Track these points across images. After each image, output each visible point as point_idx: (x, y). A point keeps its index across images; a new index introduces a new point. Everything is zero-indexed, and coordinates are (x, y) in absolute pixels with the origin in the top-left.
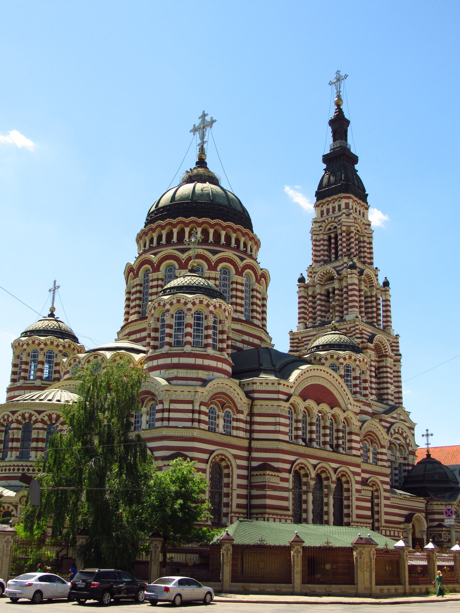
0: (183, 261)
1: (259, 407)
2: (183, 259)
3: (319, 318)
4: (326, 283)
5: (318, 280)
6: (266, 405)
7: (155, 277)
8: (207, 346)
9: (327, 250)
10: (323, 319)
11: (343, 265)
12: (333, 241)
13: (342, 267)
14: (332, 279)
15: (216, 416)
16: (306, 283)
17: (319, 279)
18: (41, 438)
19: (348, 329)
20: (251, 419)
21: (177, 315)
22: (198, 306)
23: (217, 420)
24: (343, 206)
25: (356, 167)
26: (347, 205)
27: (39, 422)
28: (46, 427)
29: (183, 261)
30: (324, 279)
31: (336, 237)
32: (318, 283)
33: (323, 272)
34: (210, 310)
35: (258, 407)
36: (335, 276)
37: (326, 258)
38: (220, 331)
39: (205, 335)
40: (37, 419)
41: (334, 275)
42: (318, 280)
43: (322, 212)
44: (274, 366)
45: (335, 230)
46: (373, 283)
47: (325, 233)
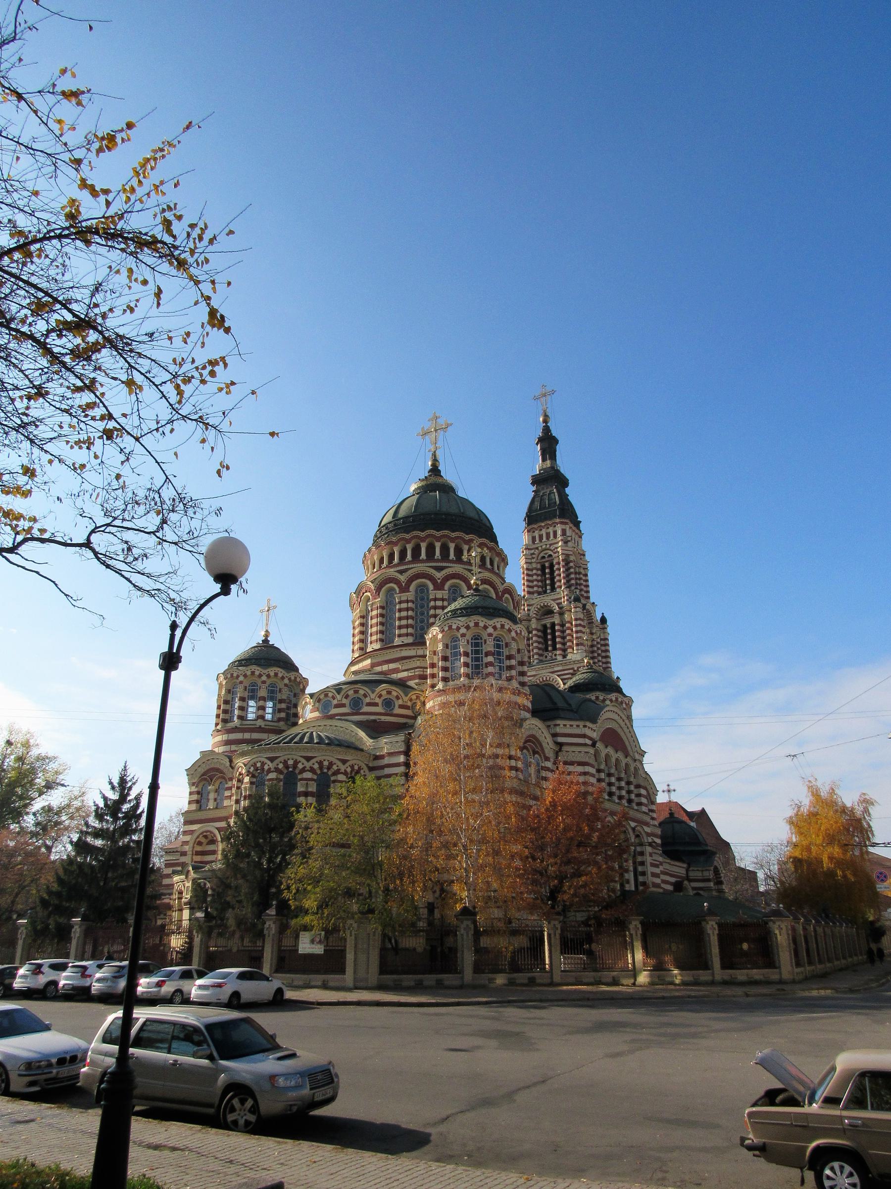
0: (439, 581)
1: (564, 753)
2: (439, 579)
3: (536, 657)
7: (403, 599)
9: (541, 581)
10: (541, 658)
12: (547, 571)
14: (549, 612)
19: (576, 669)
24: (559, 533)
25: (567, 490)
26: (564, 532)
27: (308, 770)
28: (315, 777)
29: (439, 581)
30: (540, 612)
31: (552, 566)
32: (534, 617)
37: (540, 589)
39: (507, 666)
40: (305, 767)
43: (534, 539)
44: (570, 705)
45: (550, 559)
47: (538, 561)
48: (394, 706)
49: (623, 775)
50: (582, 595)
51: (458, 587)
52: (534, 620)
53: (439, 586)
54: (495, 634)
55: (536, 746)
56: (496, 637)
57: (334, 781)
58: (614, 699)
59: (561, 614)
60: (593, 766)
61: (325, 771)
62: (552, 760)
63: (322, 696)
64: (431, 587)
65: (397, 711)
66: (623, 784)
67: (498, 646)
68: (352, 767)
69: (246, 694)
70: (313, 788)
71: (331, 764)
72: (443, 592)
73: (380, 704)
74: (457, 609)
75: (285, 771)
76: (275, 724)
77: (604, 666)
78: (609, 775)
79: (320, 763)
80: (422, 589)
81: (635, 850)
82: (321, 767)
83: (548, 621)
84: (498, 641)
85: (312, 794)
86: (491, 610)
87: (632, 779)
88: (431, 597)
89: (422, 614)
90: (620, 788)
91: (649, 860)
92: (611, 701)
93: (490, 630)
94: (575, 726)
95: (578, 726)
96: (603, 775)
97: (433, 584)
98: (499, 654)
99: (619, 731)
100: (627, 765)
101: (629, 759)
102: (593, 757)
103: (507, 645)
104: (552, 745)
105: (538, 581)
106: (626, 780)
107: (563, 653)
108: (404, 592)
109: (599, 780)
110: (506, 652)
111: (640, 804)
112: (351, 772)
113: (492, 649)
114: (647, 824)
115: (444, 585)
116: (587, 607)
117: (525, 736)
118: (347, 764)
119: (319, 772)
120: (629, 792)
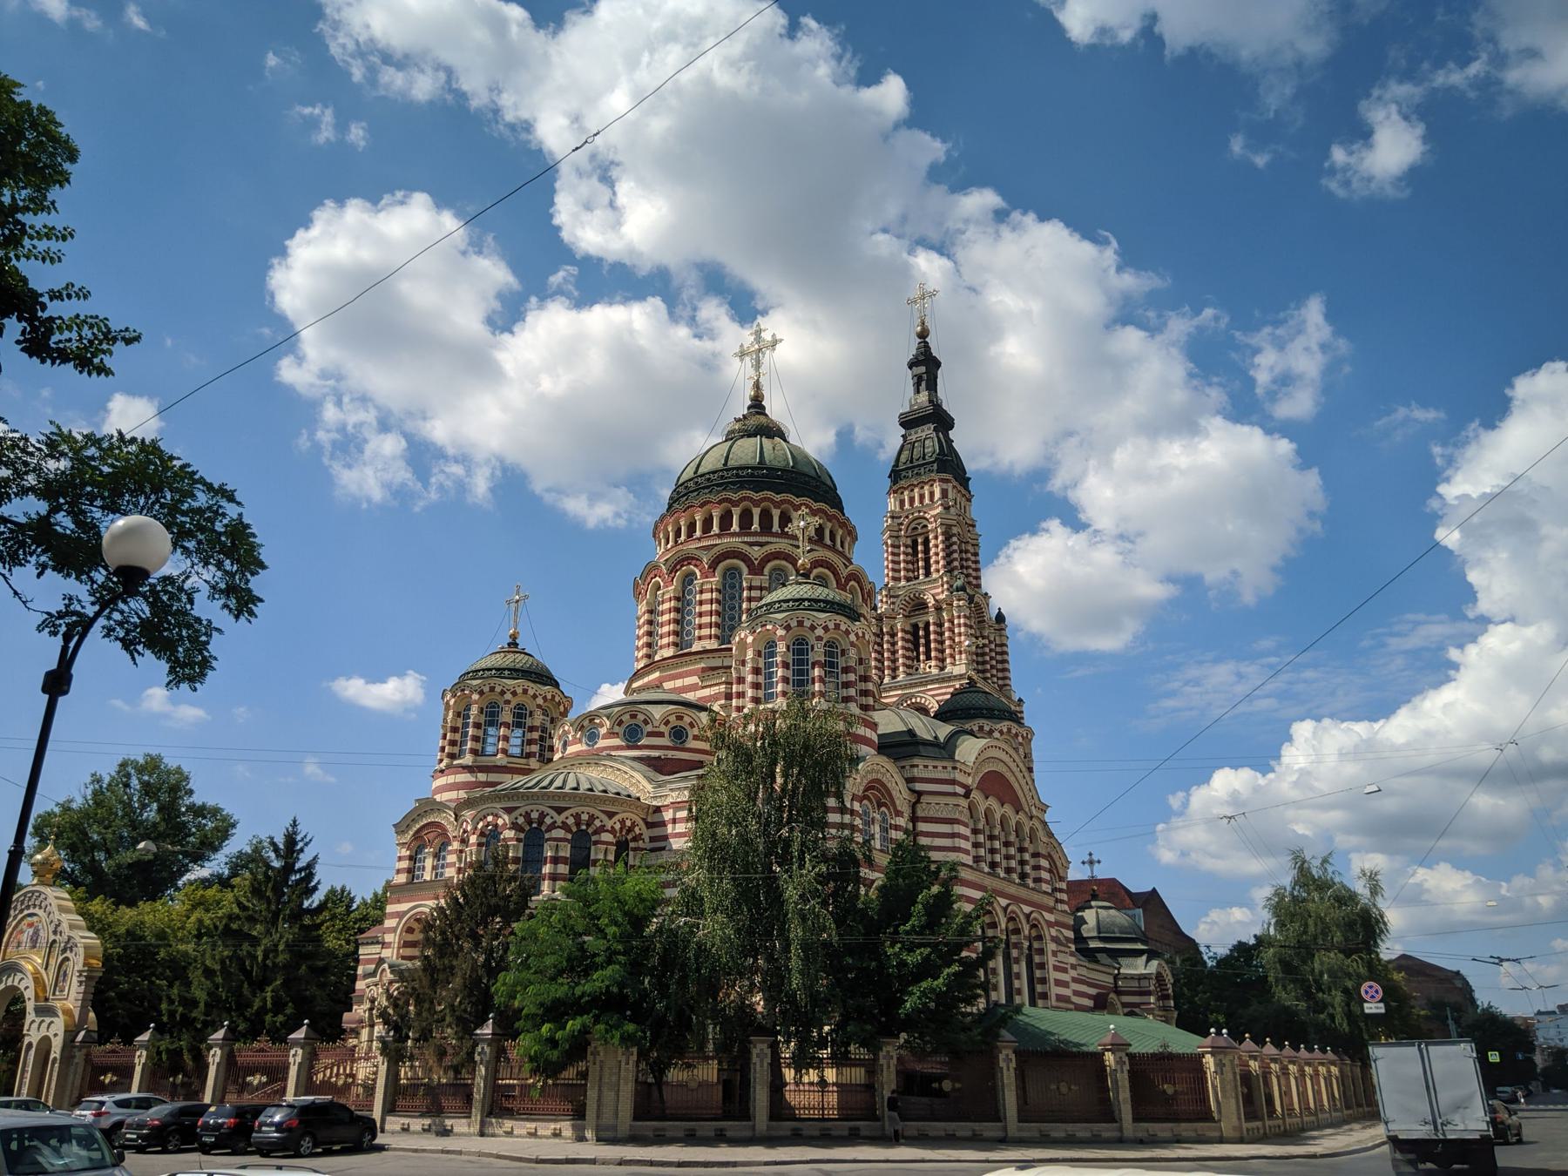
49: (1012, 838)
60: (966, 825)
63: (586, 723)
66: (1012, 851)
69: (482, 719)
73: (667, 734)
74: (775, 603)
76: (523, 761)
78: (992, 838)
81: (1030, 947)
87: (1027, 844)
90: (1008, 857)
91: (1052, 961)
93: (819, 632)
98: (832, 665)
99: (1008, 775)
100: (1018, 823)
101: (1021, 816)
102: (966, 812)
103: (843, 652)
106: (1017, 845)
110: (842, 662)
111: (1038, 880)
113: (822, 659)
114: (1051, 910)
120: (1022, 863)
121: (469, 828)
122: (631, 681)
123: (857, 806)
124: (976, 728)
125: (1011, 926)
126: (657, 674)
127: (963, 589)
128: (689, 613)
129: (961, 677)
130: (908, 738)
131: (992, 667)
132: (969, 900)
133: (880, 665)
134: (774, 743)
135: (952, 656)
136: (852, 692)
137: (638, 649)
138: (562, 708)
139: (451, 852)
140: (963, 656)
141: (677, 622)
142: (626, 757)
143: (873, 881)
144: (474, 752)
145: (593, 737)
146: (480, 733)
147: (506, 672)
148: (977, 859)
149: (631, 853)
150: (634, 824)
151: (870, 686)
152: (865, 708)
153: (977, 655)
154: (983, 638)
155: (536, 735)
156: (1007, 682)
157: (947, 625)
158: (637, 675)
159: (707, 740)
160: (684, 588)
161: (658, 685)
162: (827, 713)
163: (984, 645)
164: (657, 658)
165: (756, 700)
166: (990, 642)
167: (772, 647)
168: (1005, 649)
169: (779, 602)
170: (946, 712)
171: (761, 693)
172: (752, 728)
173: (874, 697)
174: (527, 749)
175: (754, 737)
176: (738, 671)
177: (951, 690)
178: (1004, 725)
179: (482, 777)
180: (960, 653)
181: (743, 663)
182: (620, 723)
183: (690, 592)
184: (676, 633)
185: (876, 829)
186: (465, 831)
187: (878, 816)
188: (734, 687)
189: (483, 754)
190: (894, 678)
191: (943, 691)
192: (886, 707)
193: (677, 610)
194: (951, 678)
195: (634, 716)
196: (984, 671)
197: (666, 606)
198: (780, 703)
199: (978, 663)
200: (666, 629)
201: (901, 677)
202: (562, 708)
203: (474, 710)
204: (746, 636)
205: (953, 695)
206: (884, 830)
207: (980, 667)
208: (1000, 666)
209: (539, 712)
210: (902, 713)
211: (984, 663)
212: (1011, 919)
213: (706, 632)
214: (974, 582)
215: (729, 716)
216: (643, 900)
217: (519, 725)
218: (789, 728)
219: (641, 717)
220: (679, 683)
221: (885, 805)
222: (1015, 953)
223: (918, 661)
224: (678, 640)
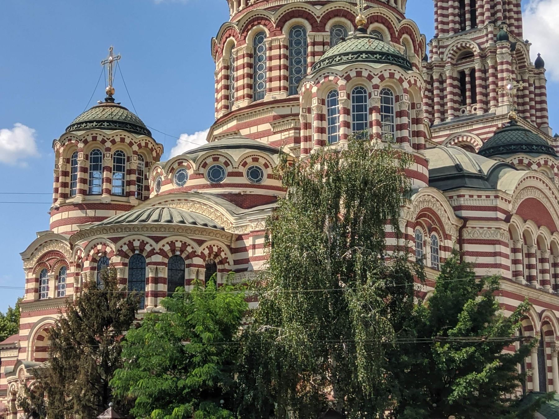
0: (318, 20)
1: (470, 230)
2: (318, 17)
4: (460, 62)
5: (449, 58)
6: (480, 228)
8: (401, 140)
10: (456, 113)
11: (487, 35)
13: (485, 39)
14: (467, 55)
15: (422, 242)
16: (429, 61)
17: (450, 55)
18: (161, 278)
20: (461, 248)
21: (355, 95)
22: (387, 81)
23: (424, 248)
27: (157, 253)
28: (166, 261)
29: (318, 20)
30: (457, 55)
33: (457, 46)
34: (405, 87)
35: (470, 231)
36: (475, 51)
37: (457, 26)
38: (413, 119)
39: (397, 125)
40: (154, 249)
41: (474, 50)
42: (449, 58)
46: (525, 62)
48: (262, 176)
49: (547, 255)
50: (512, 32)
51: (342, 27)
52: (448, 66)
53: (318, 27)
54: (382, 86)
55: (433, 221)
56: (384, 89)
57: (189, 266)
58: (542, 162)
59: (483, 57)
60: (506, 245)
61: (178, 253)
62: (454, 238)
63: (176, 166)
64: (309, 27)
65: (266, 182)
67: (386, 100)
68: (210, 248)
69: (88, 164)
70: (164, 273)
71: (185, 245)
72: (323, 33)
73: (245, 174)
74: (336, 56)
75: (131, 254)
77: (539, 121)
78: (529, 255)
79: (172, 244)
80: (297, 30)
82: (173, 250)
83: (466, 67)
84: (386, 93)
85: (163, 280)
86: (378, 56)
88: (309, 41)
89: (299, 62)
90: (543, 272)
92: (539, 165)
94: (484, 197)
95: (488, 197)
96: (519, 256)
97: (312, 24)
98: (387, 110)
99: (544, 201)
100: (553, 243)
102: (507, 234)
103: (397, 99)
104: (454, 220)
105: (454, 15)
106: (551, 261)
107: (484, 107)
108: (275, 35)
109: (515, 262)
110: (396, 107)
112: (210, 254)
113: (379, 105)
115: (325, 24)
116: (517, 47)
117: (418, 210)
118: (205, 245)
119: (170, 255)
121: (83, 255)
122: (213, 129)
123: (410, 231)
124: (516, 162)
125: (545, 329)
126: (234, 123)
127: (504, 38)
128: (261, 68)
129: (503, 117)
130: (454, 172)
131: (531, 107)
132: (509, 308)
133: (430, 109)
134: (338, 179)
135: (496, 99)
136: (405, 133)
137: (217, 101)
138: (154, 154)
139: (69, 275)
140: (505, 98)
141: (250, 76)
142: (211, 194)
143: (425, 294)
144: (83, 192)
145: (182, 178)
146: (87, 176)
147: (106, 124)
148: (516, 274)
149: (219, 274)
150: (220, 250)
151: (422, 128)
152: (417, 147)
153: (518, 97)
154: (524, 81)
155: (134, 177)
156: (545, 120)
157: (491, 71)
158: (218, 124)
159: (279, 178)
160: (255, 45)
161: (235, 132)
162: (383, 153)
163: (525, 88)
164: (234, 108)
165: (322, 143)
166: (530, 85)
167: (334, 95)
168: (543, 90)
169: (340, 55)
170: (489, 149)
171: (325, 137)
172: (318, 167)
173: (425, 137)
174: (127, 189)
175: (320, 175)
176: (305, 117)
177: (494, 129)
178: (542, 158)
179: (91, 213)
180: (503, 95)
181: (309, 110)
182: (205, 165)
183: (261, 49)
184: (250, 86)
185: (427, 250)
186: (80, 258)
187: (429, 240)
188: (302, 132)
189: (90, 194)
190: (443, 120)
191: (487, 130)
192: (435, 146)
193: (250, 66)
194: (495, 118)
195: (216, 159)
196: (524, 112)
197: (240, 62)
198: (342, 145)
199: (519, 104)
200: (240, 83)
201: (449, 119)
202: (154, 154)
203: (81, 157)
204: (311, 87)
205: (496, 133)
206: (435, 251)
207: (521, 108)
208: (538, 106)
209: (135, 157)
210: (451, 151)
211: (524, 104)
212: (545, 323)
213: (275, 84)
214: (516, 31)
215: (298, 157)
216: (231, 312)
217: (119, 169)
218: (350, 166)
219: (222, 160)
220: (254, 130)
221: (435, 230)
222: (548, 351)
223: (465, 104)
224: (251, 92)
